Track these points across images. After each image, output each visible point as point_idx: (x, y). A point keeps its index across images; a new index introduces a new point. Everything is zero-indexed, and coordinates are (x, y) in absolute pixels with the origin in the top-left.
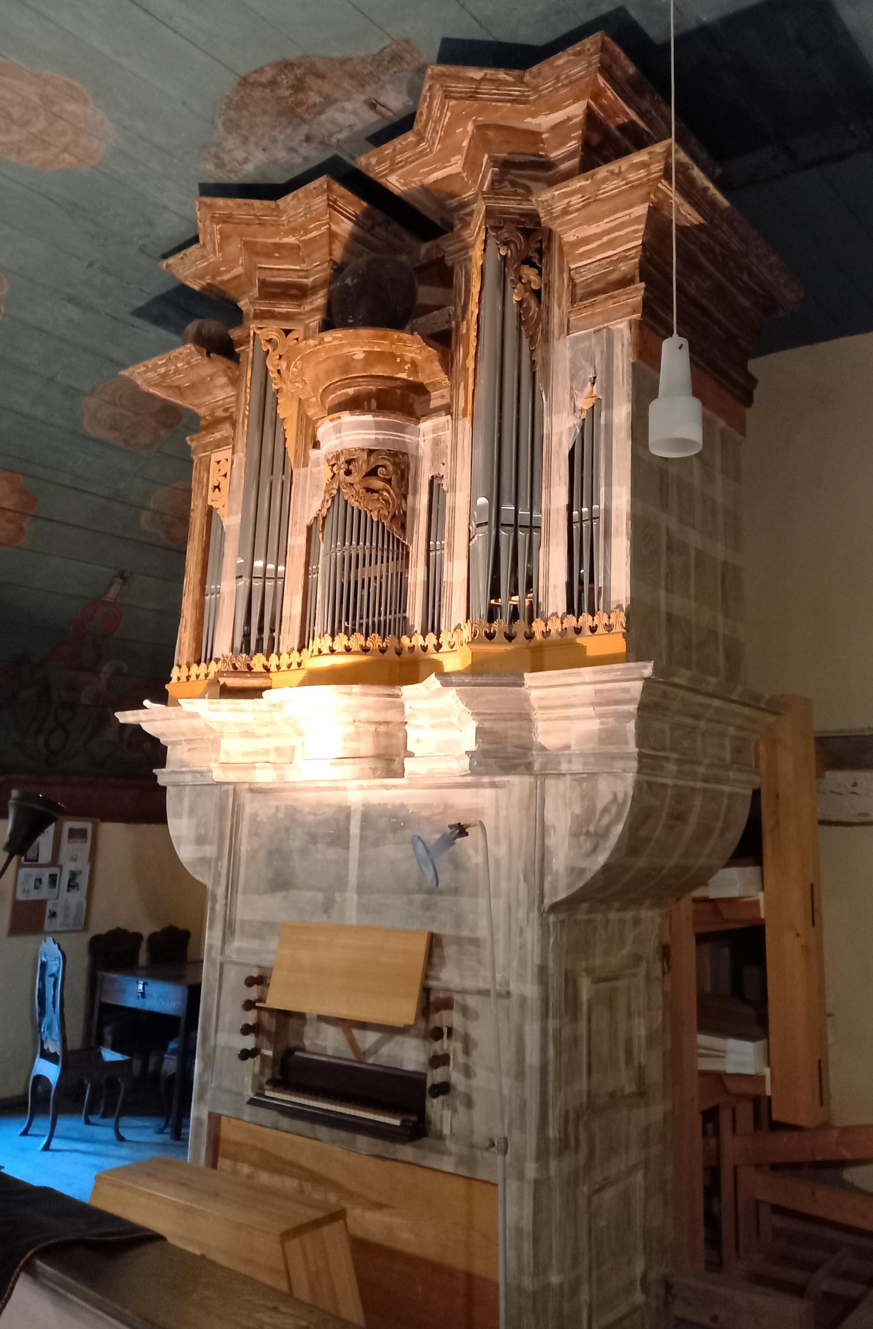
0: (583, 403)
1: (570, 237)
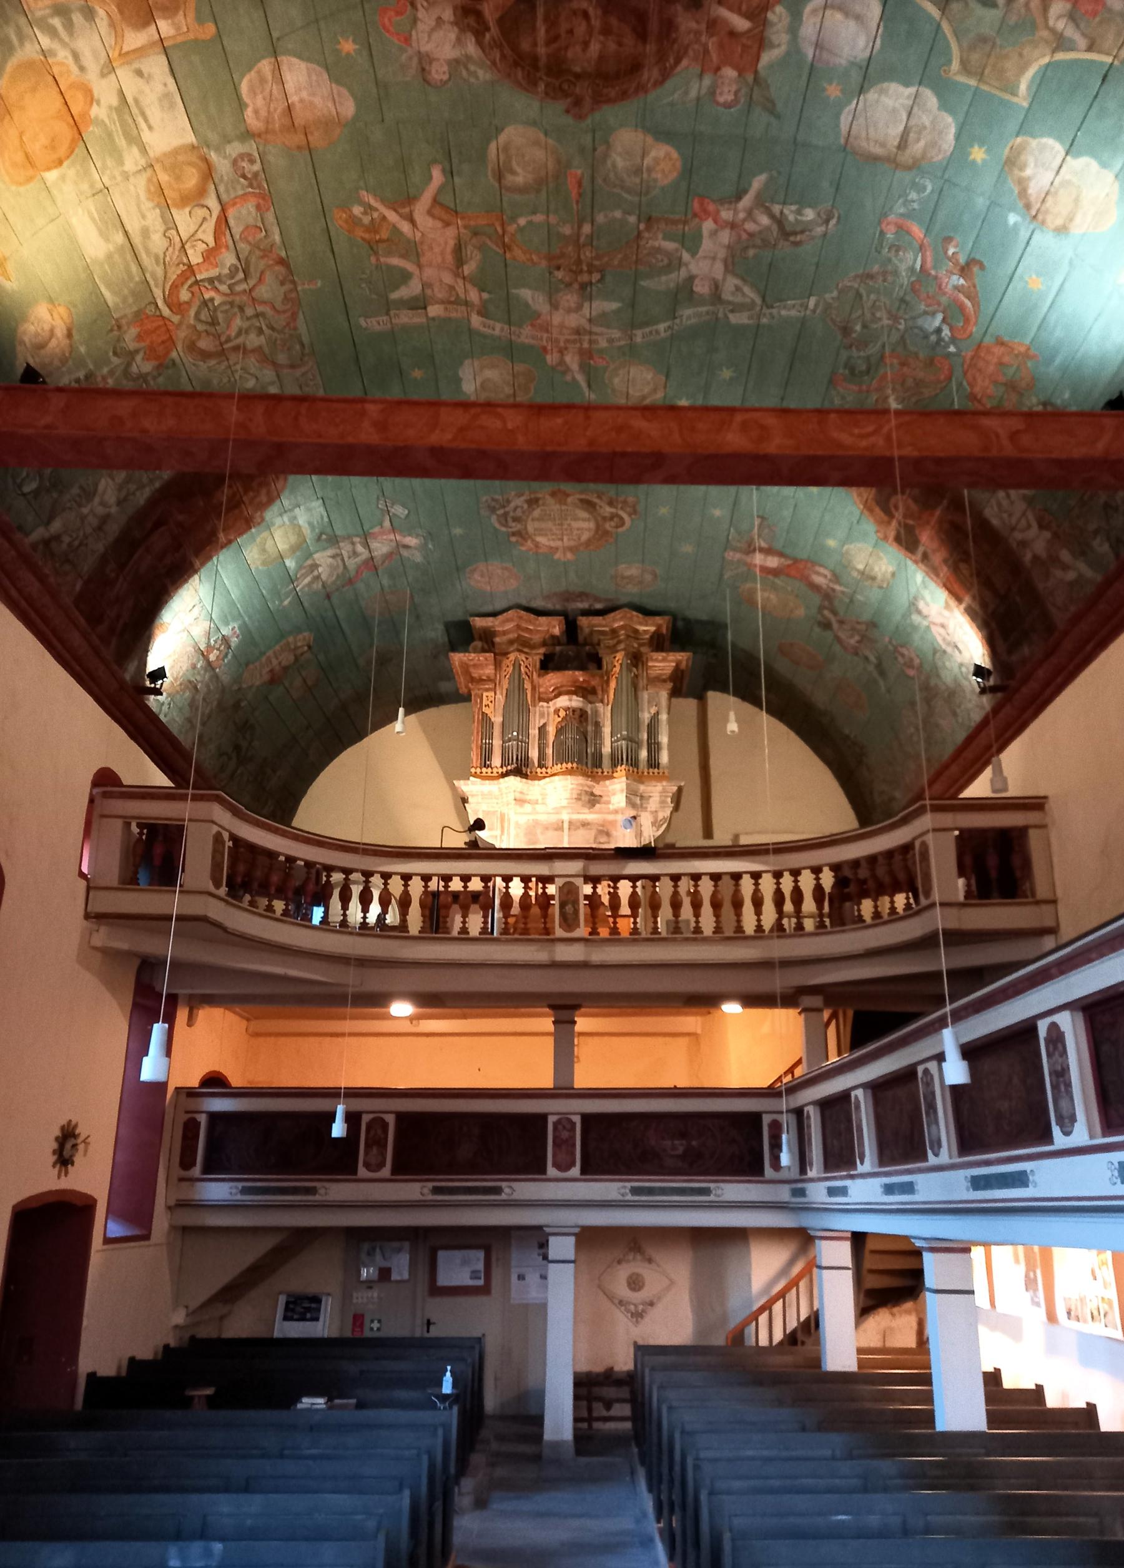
0: (653, 710)
1: (650, 664)
